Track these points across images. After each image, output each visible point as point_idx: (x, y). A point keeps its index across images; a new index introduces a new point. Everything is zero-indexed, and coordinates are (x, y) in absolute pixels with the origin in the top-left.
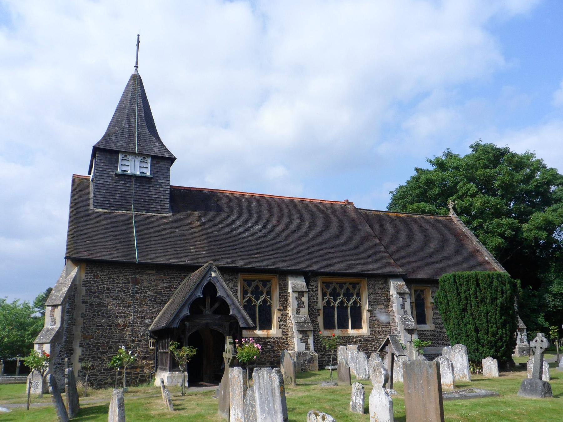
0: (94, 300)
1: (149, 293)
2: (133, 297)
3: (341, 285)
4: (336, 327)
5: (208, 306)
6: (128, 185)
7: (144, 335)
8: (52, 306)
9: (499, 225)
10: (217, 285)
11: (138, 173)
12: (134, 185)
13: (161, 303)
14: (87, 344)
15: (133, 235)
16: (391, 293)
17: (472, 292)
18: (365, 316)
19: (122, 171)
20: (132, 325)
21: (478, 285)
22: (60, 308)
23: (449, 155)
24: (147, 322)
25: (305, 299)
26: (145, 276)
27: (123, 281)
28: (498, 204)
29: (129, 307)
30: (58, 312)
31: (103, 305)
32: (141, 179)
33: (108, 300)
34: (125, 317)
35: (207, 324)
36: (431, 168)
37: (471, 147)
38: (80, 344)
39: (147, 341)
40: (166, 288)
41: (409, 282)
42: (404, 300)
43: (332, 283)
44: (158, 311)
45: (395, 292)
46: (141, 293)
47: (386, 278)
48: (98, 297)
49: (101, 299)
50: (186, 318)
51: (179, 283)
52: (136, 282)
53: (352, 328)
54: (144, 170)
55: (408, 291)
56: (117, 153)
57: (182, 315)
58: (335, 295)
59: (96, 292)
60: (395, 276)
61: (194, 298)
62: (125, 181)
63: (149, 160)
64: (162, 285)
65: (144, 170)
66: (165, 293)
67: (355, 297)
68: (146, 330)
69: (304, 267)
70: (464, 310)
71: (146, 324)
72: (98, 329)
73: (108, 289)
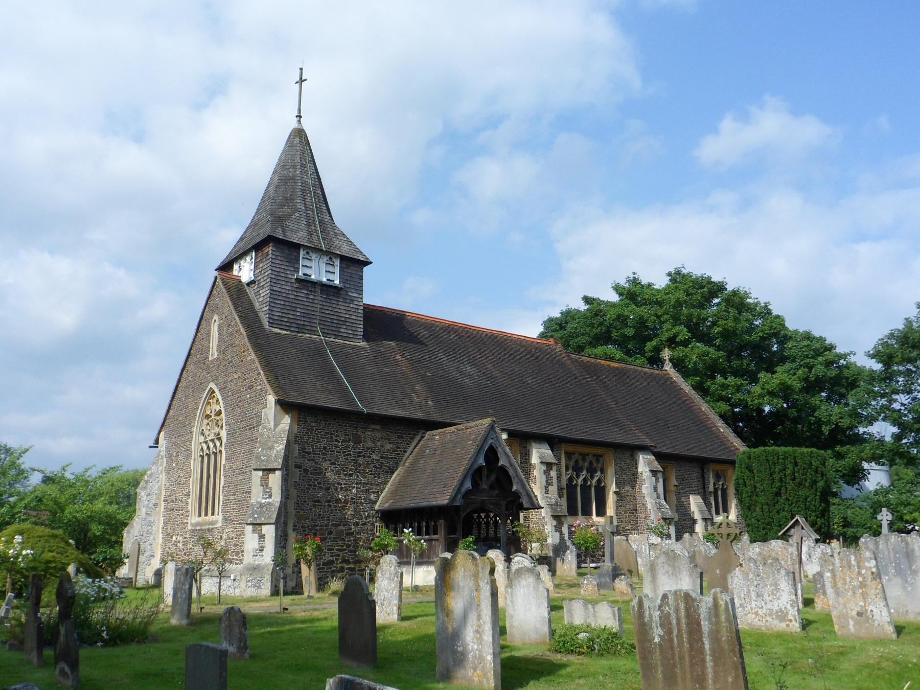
0: (308, 464)
1: (374, 456)
2: (355, 461)
3: (584, 456)
4: (580, 513)
5: (484, 479)
6: (311, 297)
7: (369, 516)
8: (264, 470)
9: (724, 387)
10: (499, 450)
11: (324, 280)
12: (319, 298)
13: (387, 472)
14: (303, 527)
15: (338, 373)
16: (640, 470)
17: (788, 472)
18: (611, 499)
19: (305, 274)
20: (354, 501)
21: (796, 464)
22: (278, 474)
23: (635, 282)
24: (372, 497)
25: (553, 474)
26: (369, 433)
27: (343, 438)
28: (720, 358)
29: (351, 475)
30: (275, 480)
31: (320, 472)
32: (327, 289)
33: (325, 465)
34: (347, 490)
35: (483, 501)
36: (614, 298)
37: (669, 274)
38: (294, 526)
39: (373, 525)
40: (394, 451)
41: (659, 457)
42: (657, 481)
43: (588, 455)
44: (386, 483)
45: (647, 469)
46: (364, 456)
47: (633, 450)
48: (313, 460)
49: (316, 463)
50: (468, 492)
52: (357, 441)
53: (598, 515)
54: (331, 277)
55: (661, 469)
56: (296, 247)
57: (463, 490)
58: (577, 470)
59: (310, 453)
60: (644, 449)
61: (476, 466)
62: (308, 290)
63: (337, 262)
64: (389, 446)
65: (331, 277)
67: (599, 473)
68: (372, 508)
69: (547, 430)
70: (778, 494)
71: (370, 500)
72: (315, 506)
73: (325, 448)
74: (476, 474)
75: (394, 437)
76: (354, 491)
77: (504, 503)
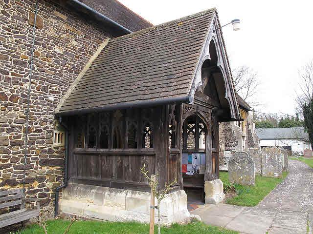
1: (57, 49)
7: (45, 121)
24: (51, 98)
27: (15, 13)
75: (81, 35)
76: (27, 86)
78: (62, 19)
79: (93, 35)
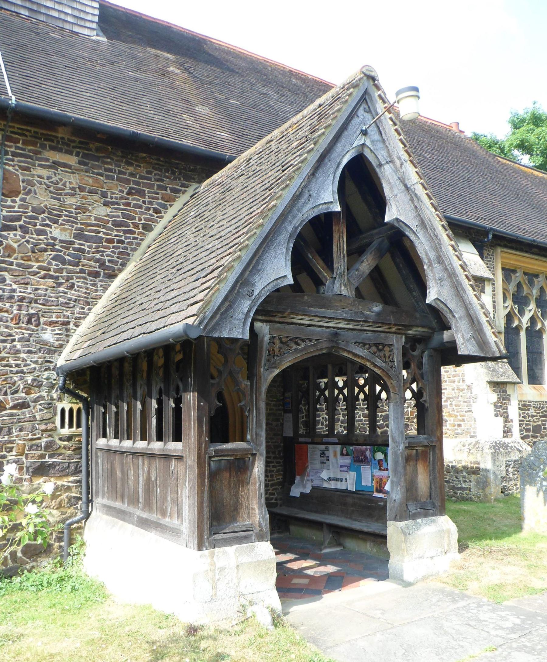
1: (56, 232)
5: (340, 263)
7: (37, 384)
13: (96, 275)
26: (45, 173)
35: (335, 334)
39: (50, 406)
40: (116, 224)
44: (89, 302)
46: (25, 230)
51: (157, 211)
61: (307, 212)
64: (102, 211)
66: (110, 241)
74: (313, 243)
75: (117, 191)
77: (397, 343)
78: (65, 165)
79: (151, 186)
